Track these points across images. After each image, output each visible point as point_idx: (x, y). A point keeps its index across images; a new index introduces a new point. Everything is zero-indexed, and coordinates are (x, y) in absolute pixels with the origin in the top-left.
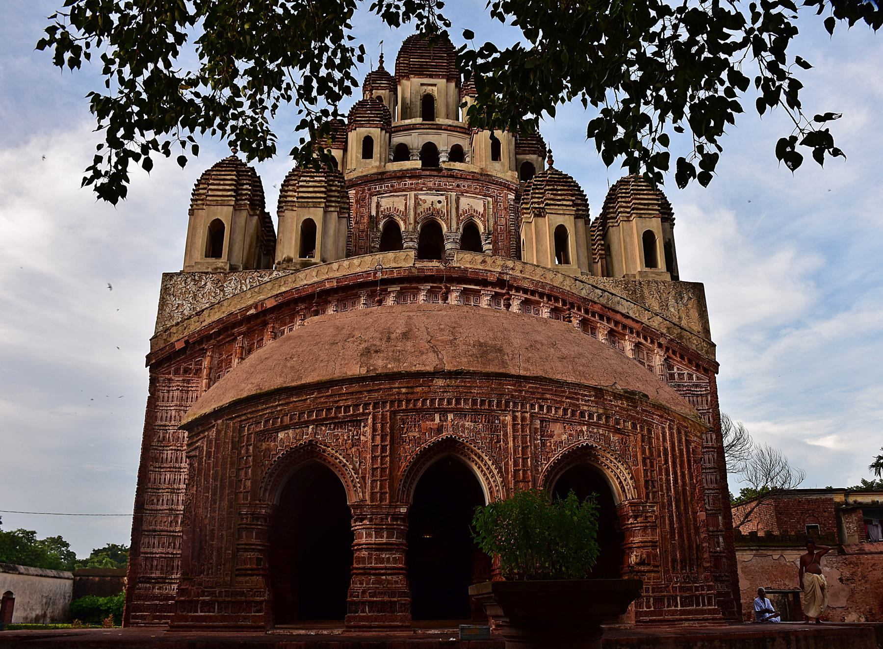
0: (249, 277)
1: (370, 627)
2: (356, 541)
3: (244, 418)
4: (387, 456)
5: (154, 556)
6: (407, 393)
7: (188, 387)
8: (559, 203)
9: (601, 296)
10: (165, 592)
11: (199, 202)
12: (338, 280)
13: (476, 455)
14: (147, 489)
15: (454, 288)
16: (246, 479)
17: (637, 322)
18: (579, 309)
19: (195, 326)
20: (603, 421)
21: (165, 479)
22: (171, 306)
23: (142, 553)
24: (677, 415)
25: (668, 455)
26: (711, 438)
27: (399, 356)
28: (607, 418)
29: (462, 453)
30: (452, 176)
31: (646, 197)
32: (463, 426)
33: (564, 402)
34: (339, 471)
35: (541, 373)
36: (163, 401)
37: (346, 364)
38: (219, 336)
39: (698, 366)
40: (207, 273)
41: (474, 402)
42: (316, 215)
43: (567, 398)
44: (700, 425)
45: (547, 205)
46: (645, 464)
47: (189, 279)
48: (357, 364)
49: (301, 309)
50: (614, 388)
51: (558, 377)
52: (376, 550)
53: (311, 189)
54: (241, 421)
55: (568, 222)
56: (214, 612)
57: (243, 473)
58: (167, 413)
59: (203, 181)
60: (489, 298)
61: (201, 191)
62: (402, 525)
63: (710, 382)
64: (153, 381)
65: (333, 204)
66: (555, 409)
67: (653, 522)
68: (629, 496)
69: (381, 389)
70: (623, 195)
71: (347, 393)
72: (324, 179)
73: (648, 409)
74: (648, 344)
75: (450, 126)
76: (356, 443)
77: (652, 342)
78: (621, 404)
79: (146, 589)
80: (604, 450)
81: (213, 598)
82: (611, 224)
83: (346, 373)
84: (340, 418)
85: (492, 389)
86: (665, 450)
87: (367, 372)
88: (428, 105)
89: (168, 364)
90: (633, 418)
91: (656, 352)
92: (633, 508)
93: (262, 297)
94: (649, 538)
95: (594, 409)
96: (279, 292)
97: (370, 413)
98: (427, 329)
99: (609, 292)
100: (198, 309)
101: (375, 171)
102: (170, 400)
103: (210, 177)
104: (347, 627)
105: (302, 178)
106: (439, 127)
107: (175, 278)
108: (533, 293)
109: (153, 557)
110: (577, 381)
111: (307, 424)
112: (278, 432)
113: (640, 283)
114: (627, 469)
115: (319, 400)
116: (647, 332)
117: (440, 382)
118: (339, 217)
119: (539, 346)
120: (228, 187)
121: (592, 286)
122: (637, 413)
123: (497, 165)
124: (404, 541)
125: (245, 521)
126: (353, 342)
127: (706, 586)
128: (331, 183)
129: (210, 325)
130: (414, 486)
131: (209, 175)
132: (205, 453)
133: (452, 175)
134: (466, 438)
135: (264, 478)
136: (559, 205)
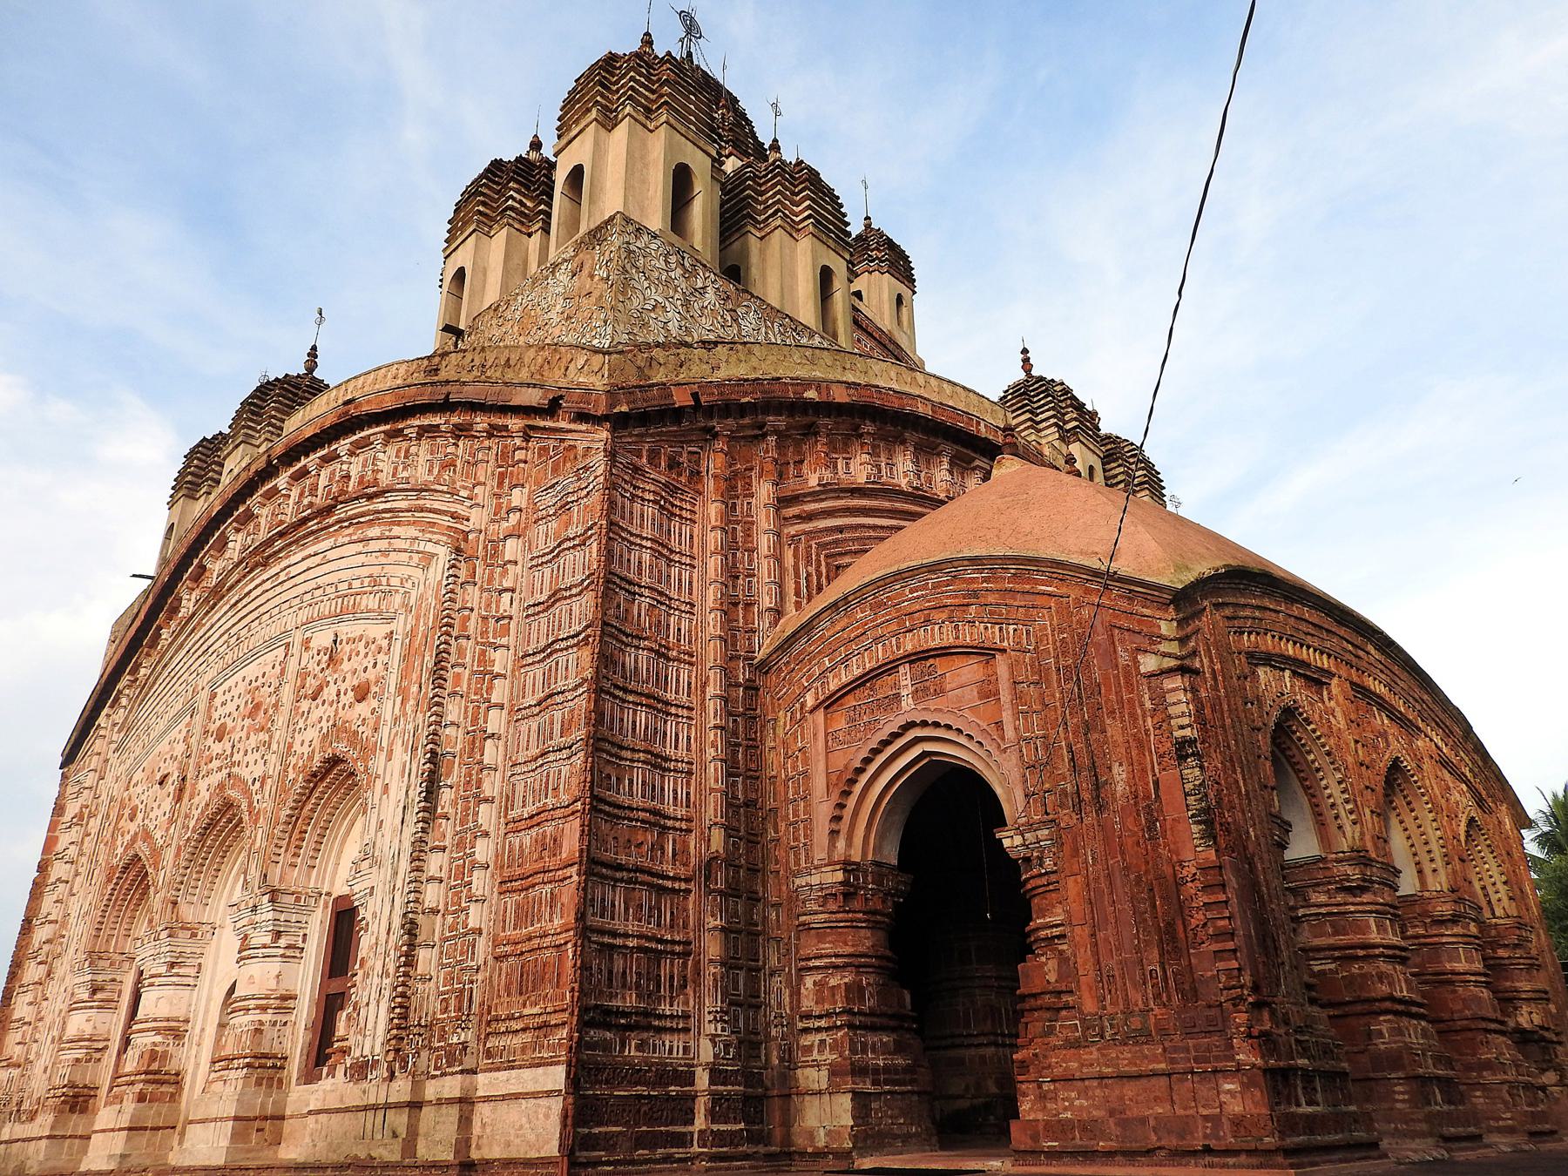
5: (619, 941)
38: (742, 417)
49: (868, 433)
109: (612, 947)
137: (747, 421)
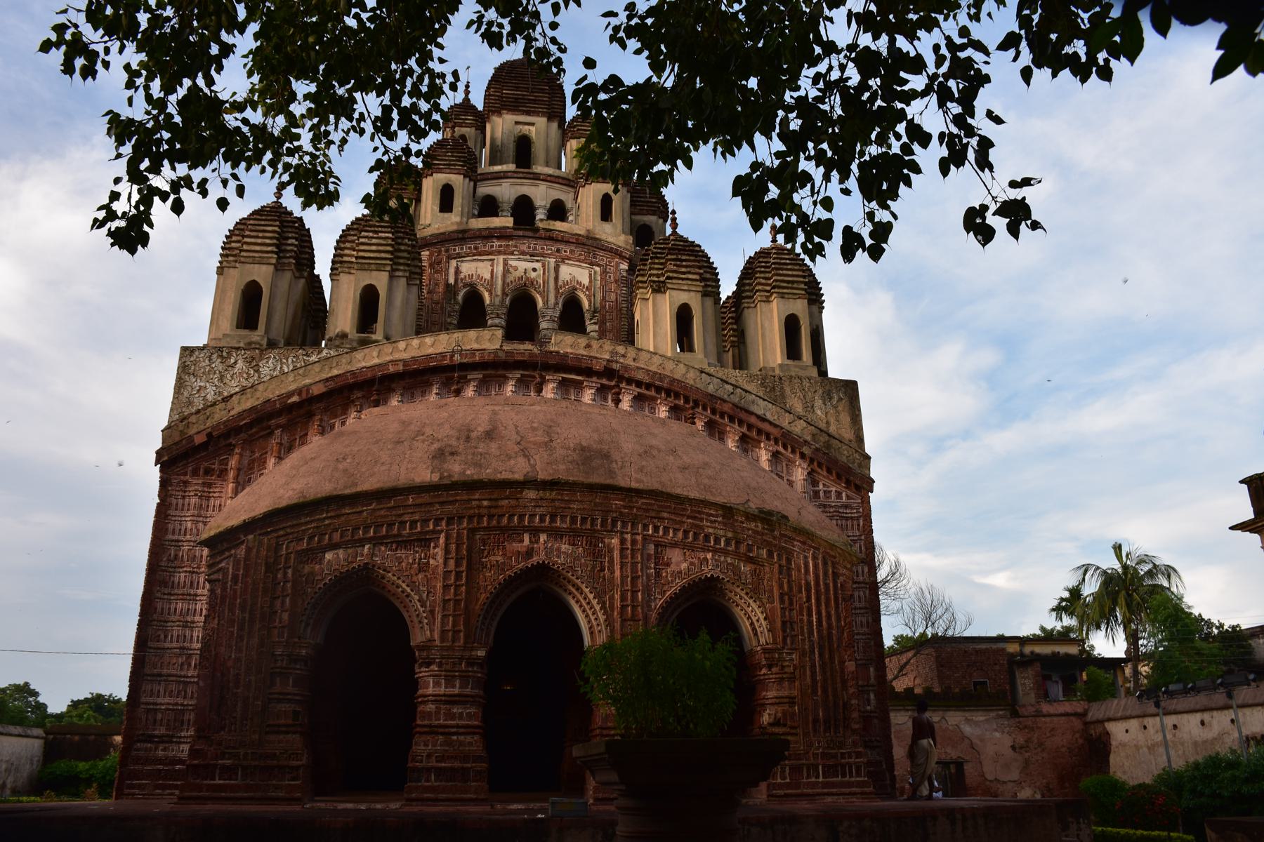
0: (292, 355)
1: (437, 800)
2: (420, 692)
3: (281, 533)
4: (463, 585)
5: (158, 707)
6: (490, 507)
7: (210, 492)
8: (683, 276)
9: (732, 393)
10: (171, 754)
11: (231, 258)
12: (405, 362)
13: (573, 586)
14: (152, 621)
15: (551, 377)
16: (282, 611)
17: (776, 426)
18: (705, 409)
19: (220, 415)
20: (731, 548)
21: (176, 609)
22: (189, 389)
23: (143, 704)
24: (822, 542)
25: (811, 591)
26: (863, 572)
27: (480, 460)
28: (738, 543)
29: (556, 584)
30: (551, 239)
31: (790, 273)
32: (559, 549)
33: (684, 522)
34: (402, 603)
35: (656, 486)
36: (176, 509)
37: (414, 468)
38: (251, 429)
39: (848, 483)
40: (238, 349)
41: (573, 520)
42: (380, 280)
43: (689, 517)
44: (850, 554)
45: (668, 278)
46: (782, 601)
47: (215, 356)
48: (427, 468)
49: (358, 398)
50: (746, 506)
51: (678, 491)
52: (446, 702)
53: (374, 248)
54: (278, 537)
55: (693, 299)
56: (237, 780)
57: (278, 603)
58: (181, 525)
59: (237, 232)
60: (593, 391)
61: (233, 245)
62: (478, 672)
63: (862, 502)
64: (164, 483)
65: (402, 268)
66: (673, 531)
67: (791, 673)
68: (762, 641)
69: (457, 501)
70: (763, 269)
71: (414, 505)
72: (390, 235)
73: (787, 533)
74: (788, 454)
75: (550, 175)
76: (423, 568)
77: (793, 452)
78: (755, 526)
79: (146, 749)
80: (733, 584)
81: (236, 762)
82: (746, 305)
83: (413, 480)
84: (404, 536)
85: (596, 505)
86: (808, 584)
87: (440, 478)
88: (523, 150)
89: (185, 462)
90: (769, 543)
91: (797, 463)
92: (767, 655)
93: (307, 381)
94: (786, 693)
95: (721, 533)
96: (330, 375)
97: (442, 531)
98: (516, 427)
99: (742, 389)
100: (226, 394)
101: (455, 228)
102: (186, 508)
103: (245, 227)
104: (408, 800)
105: (363, 233)
106: (537, 177)
107: (197, 353)
108: (648, 386)
109: (156, 709)
110: (702, 497)
111: (362, 543)
112: (324, 552)
113: (780, 379)
114: (759, 607)
115: (378, 513)
116: (787, 440)
117: (531, 494)
118: (408, 284)
119: (655, 452)
120: (268, 241)
121: (722, 380)
122: (774, 538)
123: (607, 227)
124: (481, 693)
125: (279, 664)
126: (423, 441)
127: (854, 752)
128: (400, 241)
129: (240, 414)
130: (495, 624)
131: (245, 224)
132: (230, 576)
133: (551, 237)
134: (562, 564)
135: (306, 609)
136: (683, 279)
137: (254, 430)
